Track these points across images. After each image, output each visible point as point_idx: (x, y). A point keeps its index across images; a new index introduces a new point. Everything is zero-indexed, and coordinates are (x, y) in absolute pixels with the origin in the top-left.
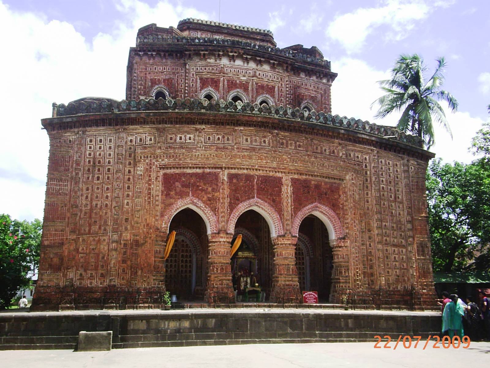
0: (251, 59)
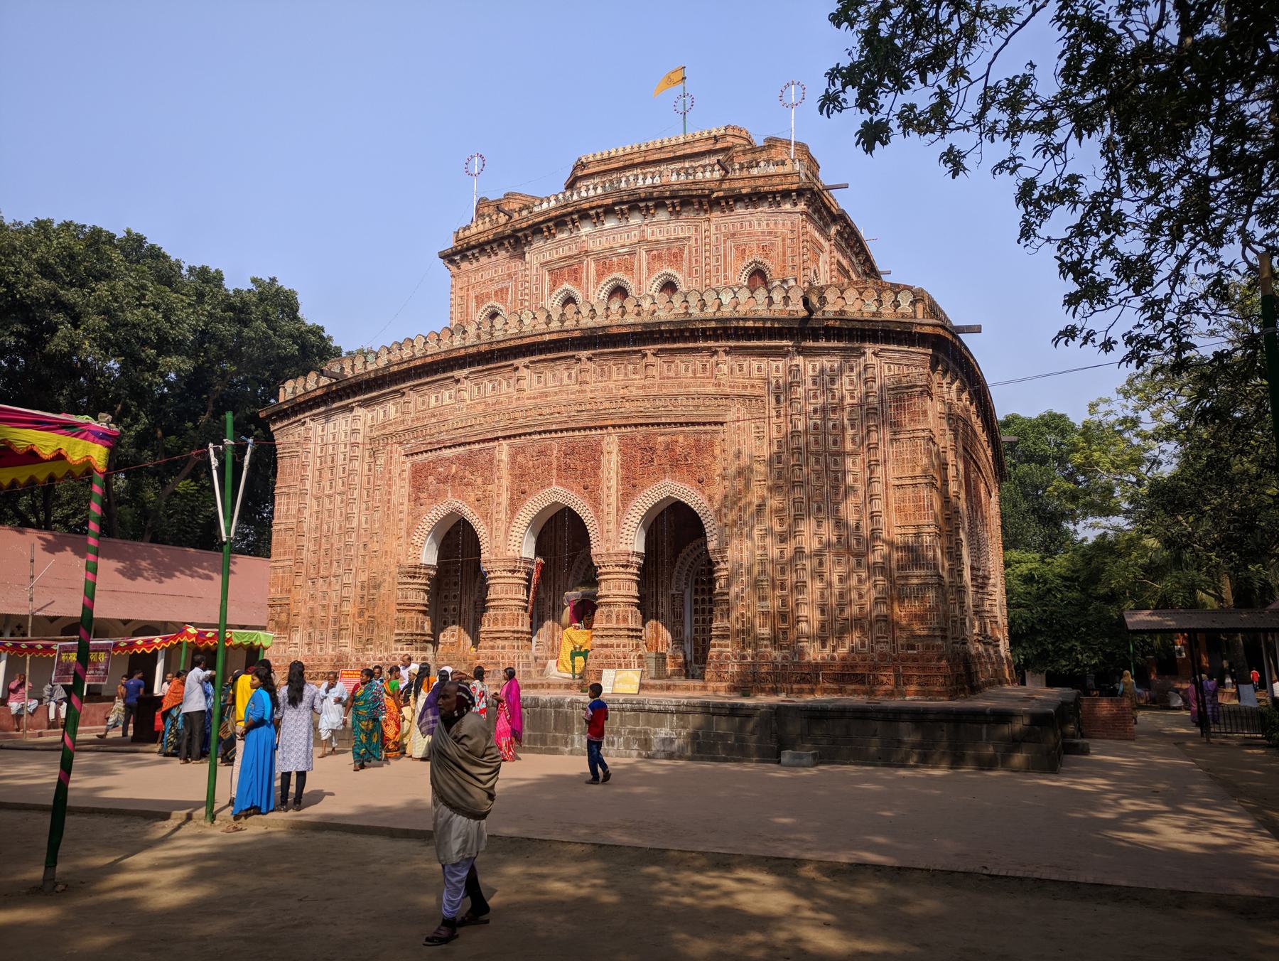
0: (631, 209)
